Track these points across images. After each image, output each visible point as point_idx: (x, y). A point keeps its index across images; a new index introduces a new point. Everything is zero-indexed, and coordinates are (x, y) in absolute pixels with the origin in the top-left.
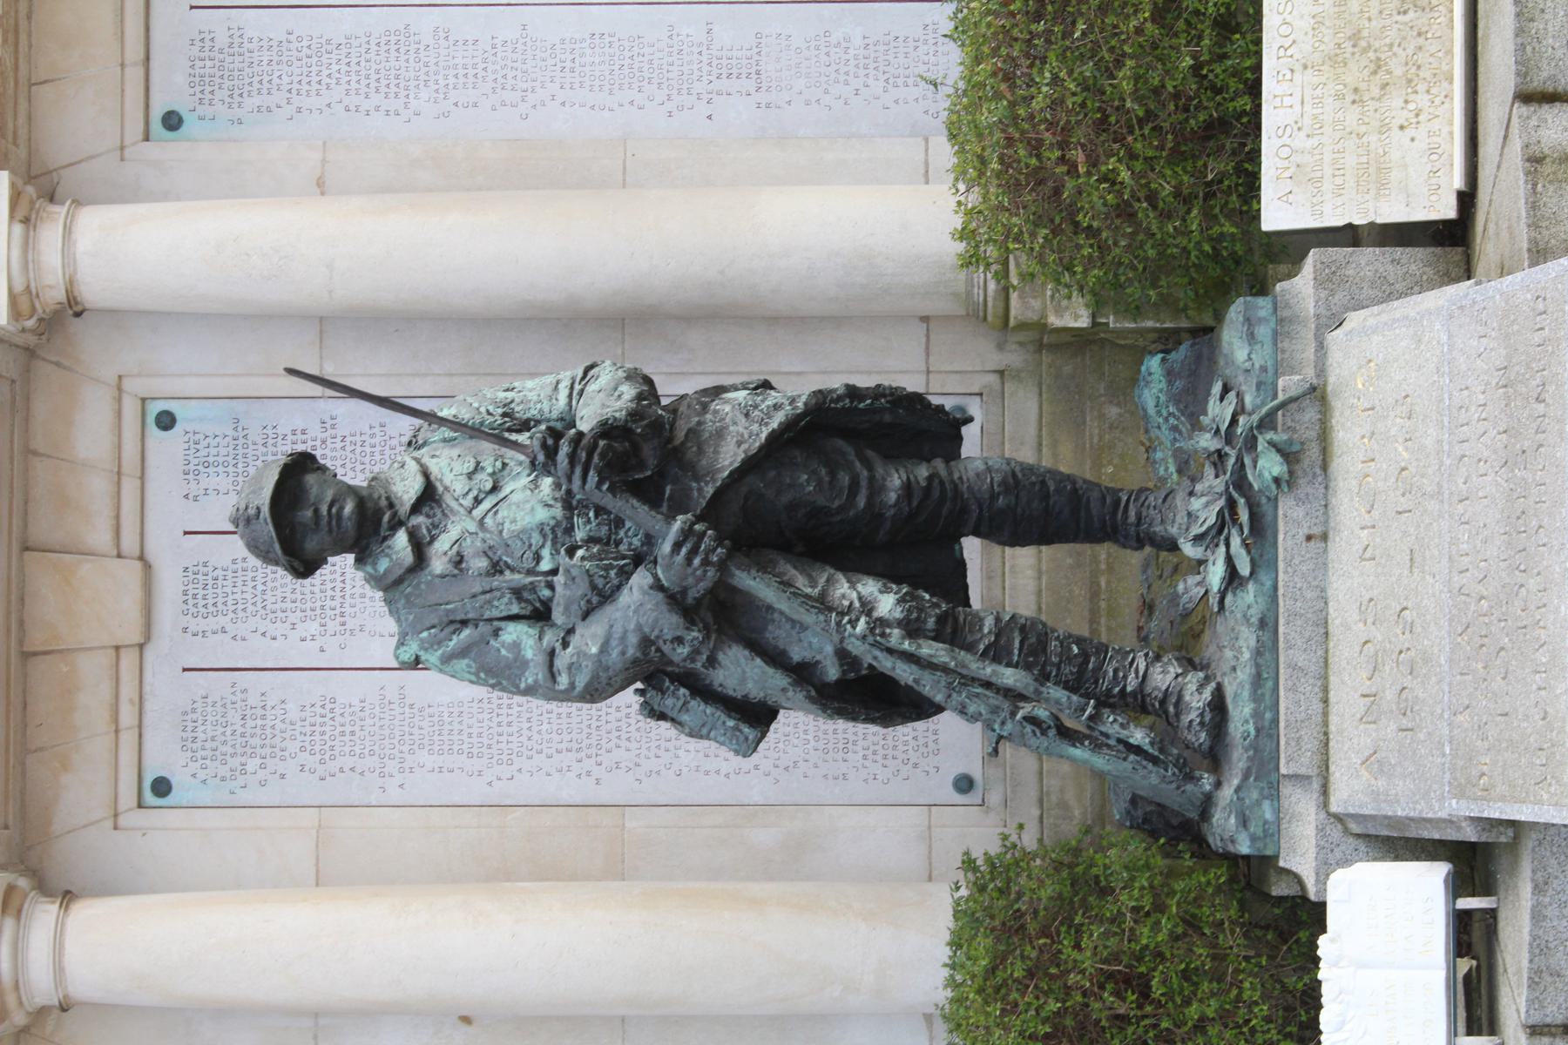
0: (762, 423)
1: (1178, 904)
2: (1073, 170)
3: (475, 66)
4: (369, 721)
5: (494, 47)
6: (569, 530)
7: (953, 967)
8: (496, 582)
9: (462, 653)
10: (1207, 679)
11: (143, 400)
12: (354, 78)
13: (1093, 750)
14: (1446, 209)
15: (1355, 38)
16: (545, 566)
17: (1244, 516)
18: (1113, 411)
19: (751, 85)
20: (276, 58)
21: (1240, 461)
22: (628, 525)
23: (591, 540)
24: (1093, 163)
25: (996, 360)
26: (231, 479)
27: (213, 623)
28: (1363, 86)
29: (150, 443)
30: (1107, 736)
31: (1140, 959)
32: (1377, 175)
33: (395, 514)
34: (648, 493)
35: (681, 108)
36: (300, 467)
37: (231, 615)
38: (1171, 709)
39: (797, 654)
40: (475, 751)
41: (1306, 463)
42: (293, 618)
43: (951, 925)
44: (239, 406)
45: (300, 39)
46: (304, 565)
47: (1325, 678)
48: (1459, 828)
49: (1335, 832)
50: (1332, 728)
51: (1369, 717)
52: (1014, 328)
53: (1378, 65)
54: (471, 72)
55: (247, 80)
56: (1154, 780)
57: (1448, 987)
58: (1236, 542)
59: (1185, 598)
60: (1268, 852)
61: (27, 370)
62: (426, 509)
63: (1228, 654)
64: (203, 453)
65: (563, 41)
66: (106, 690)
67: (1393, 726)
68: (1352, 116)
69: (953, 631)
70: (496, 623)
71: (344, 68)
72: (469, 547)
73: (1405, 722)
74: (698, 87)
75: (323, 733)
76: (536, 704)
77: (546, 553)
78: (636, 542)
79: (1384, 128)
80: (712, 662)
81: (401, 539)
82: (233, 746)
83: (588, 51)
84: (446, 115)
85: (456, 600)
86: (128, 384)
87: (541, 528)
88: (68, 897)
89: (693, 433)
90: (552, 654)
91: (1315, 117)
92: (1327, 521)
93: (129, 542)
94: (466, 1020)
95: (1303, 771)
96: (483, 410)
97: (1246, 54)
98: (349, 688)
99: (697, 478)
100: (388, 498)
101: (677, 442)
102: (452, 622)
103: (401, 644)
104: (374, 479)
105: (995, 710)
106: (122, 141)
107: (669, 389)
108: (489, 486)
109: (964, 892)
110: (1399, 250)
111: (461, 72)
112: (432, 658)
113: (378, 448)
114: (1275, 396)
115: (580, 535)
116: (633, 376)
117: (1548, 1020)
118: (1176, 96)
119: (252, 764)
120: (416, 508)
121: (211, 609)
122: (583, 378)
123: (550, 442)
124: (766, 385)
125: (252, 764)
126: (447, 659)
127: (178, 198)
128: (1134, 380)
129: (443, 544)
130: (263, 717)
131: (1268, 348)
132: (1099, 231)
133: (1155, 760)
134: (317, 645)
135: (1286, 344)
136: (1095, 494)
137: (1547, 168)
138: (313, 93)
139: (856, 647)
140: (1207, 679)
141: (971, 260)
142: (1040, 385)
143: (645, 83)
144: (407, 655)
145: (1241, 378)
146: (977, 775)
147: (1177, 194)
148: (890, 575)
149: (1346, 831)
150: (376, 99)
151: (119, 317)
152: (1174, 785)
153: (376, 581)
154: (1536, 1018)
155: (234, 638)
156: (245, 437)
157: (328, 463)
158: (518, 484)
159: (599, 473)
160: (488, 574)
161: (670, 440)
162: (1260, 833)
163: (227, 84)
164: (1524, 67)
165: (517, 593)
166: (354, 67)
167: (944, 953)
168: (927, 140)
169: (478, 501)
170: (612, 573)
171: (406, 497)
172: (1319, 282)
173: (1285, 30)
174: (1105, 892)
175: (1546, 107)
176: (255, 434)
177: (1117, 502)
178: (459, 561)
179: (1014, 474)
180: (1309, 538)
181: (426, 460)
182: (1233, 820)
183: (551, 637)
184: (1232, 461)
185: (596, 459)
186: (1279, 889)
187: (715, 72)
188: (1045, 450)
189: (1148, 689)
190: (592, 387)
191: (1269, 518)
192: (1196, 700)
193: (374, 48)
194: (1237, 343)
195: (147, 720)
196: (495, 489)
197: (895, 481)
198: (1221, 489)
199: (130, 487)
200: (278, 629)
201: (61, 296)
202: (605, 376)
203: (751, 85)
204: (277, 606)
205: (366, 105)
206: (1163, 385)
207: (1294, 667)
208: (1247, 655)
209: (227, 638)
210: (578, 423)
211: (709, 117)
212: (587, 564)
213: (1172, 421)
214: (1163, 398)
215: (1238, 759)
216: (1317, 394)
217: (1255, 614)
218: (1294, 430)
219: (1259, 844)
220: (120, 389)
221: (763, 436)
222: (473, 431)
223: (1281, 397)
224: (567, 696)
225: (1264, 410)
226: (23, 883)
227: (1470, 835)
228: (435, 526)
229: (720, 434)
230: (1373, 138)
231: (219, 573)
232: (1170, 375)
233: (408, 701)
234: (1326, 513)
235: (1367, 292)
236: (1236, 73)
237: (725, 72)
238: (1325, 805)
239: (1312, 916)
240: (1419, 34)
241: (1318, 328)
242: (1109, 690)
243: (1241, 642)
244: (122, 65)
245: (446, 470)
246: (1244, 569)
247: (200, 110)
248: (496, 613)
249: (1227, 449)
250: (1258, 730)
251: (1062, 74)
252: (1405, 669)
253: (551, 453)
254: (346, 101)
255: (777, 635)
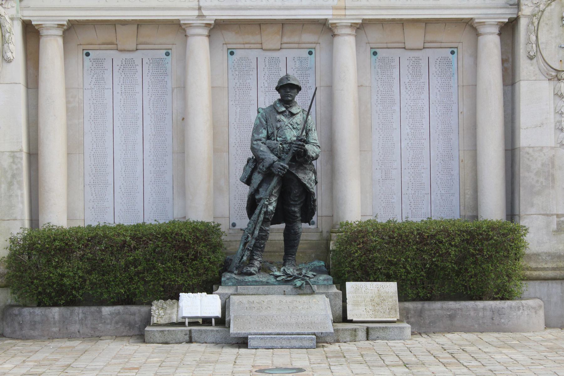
0: (308, 182)
1: (211, 267)
2: (358, 245)
3: (387, 118)
4: (246, 97)
5: (391, 122)
6: (285, 144)
7: (197, 222)
8: (275, 129)
9: (261, 122)
10: (256, 272)
11: (315, 48)
12: (384, 93)
13: (242, 249)
14: (349, 317)
15: (384, 300)
16: (278, 139)
17: (289, 279)
18: (313, 256)
19: (384, 178)
20: (389, 76)
21: (300, 278)
22: (287, 155)
23: (283, 148)
24: (360, 249)
25: (325, 231)
26: (298, 67)
27: (267, 63)
28: (374, 301)
29: (306, 50)
30: (245, 252)
31: (200, 259)
32: (357, 304)
33: (289, 108)
34: (293, 159)
35: (378, 163)
36: (298, 88)
37: (269, 68)
38: (250, 265)
39: (261, 190)
40: (240, 120)
41: (299, 291)
42: (268, 81)
43: (206, 222)
44: (314, 69)
45: (393, 81)
46: (278, 89)
47: (257, 294)
48: (228, 317)
49: (226, 297)
50: (247, 296)
51: (249, 302)
52: (330, 235)
53: (378, 304)
54: (386, 118)
55: (384, 69)
56: (236, 261)
57: (197, 317)
58: (284, 277)
59: (272, 268)
60: (222, 284)
61: (321, 24)
62: (290, 114)
63: (261, 276)
64: (304, 61)
65: (393, 137)
66: (253, 41)
67: (247, 306)
68: (368, 299)
69: (266, 221)
70: (267, 129)
71: (387, 90)
72: (282, 123)
73: (248, 308)
74: (383, 166)
75: (244, 87)
76: (250, 137)
77: (281, 139)
78: (283, 157)
79: (366, 305)
80: (259, 173)
81: (284, 109)
82: (241, 69)
83: (391, 143)
84: (377, 112)
85: (271, 121)
86: (318, 45)
87: (286, 138)
88: (209, 36)
89: (306, 168)
90: (260, 140)
91: (368, 292)
92: (287, 294)
93: (284, 46)
94: (183, 119)
95: (238, 290)
96: (310, 125)
97: (382, 279)
98: (253, 93)
99: (296, 169)
100: (292, 106)
101: (303, 165)
102: (267, 120)
103: (262, 109)
104: (296, 102)
105: (250, 230)
106: (371, 43)
107: (314, 162)
108: (294, 127)
109: (213, 224)
110: (342, 309)
111: (386, 116)
112: (260, 116)
113: (305, 99)
114: (312, 285)
115: (284, 146)
116: (317, 156)
117: (192, 333)
118: (373, 265)
119: (237, 73)
120: (290, 112)
121: (270, 63)
122: (317, 145)
123: (303, 140)
124: (316, 183)
125: (237, 73)
126: (259, 118)
127: (357, 55)
128: (320, 260)
129: (282, 118)
130: (247, 75)
131: (322, 283)
132: (346, 250)
133: (240, 262)
134: (263, 86)
135: (323, 287)
136: (294, 251)
137: (354, 333)
138: (381, 84)
139: (262, 202)
140: (256, 272)
141: (342, 225)
142: (319, 240)
143: (384, 155)
144: (260, 110)
145: (316, 278)
146: (237, 227)
147: (354, 266)
148: (277, 208)
149: (227, 299)
150: (380, 97)
151: (331, 44)
152: (235, 265)
153: (275, 103)
154: (193, 331)
155: (264, 68)
156: (307, 70)
157: (299, 93)
158: (295, 133)
159: (297, 150)
160: (277, 127)
161: (304, 164)
162: (226, 282)
163: (383, 65)
164: (372, 328)
165: (273, 133)
166: (387, 92)
167: (200, 220)
168: (372, 216)
169: (291, 125)
170: (277, 152)
171: (292, 110)
172: (335, 293)
173: (386, 286)
174: (213, 252)
175: (366, 333)
176: (308, 72)
177: (293, 255)
178: (279, 121)
179: (298, 234)
180: (284, 291)
181: (300, 113)
182: (228, 277)
183: (264, 140)
184: (300, 276)
185: (299, 149)
186: (214, 287)
187: (386, 170)
188: (305, 241)
189: (254, 261)
190: (315, 147)
191: (288, 284)
192: (252, 270)
193: (391, 97)
194: (323, 277)
195: (247, 50)
196: (294, 128)
197: (296, 209)
198: (294, 274)
199: (296, 46)
200: (266, 78)
201: (336, 33)
202: (317, 150)
203: (384, 178)
204: (271, 78)
205: (379, 95)
206: (318, 265)
207: (259, 288)
208: (261, 279)
209: (264, 67)
210: (307, 145)
211: (377, 169)
212: (278, 147)
213: (310, 267)
214: (315, 265)
215: (240, 278)
216: (313, 293)
217: (269, 281)
218: (306, 288)
219: (224, 282)
220: (317, 43)
221: (305, 182)
222: (306, 122)
223: (312, 286)
224: (252, 143)
225: (309, 282)
226: (212, 27)
227: (227, 319)
228: (286, 116)
229: (305, 174)
230: (364, 304)
231: (278, 65)
232: (320, 266)
233: (251, 106)
234: (289, 294)
235: (333, 303)
236: (378, 277)
237: (387, 172)
238: (232, 295)
239: (210, 292)
240: (384, 312)
241: (326, 293)
242: (254, 253)
243: (264, 279)
244: (387, 43)
245: (297, 118)
246: (278, 279)
247: (377, 60)
248: (269, 129)
249: (302, 276)
250: (246, 282)
251: (377, 242)
252: (258, 308)
253: (300, 140)
254: (380, 91)
255: (265, 186)
